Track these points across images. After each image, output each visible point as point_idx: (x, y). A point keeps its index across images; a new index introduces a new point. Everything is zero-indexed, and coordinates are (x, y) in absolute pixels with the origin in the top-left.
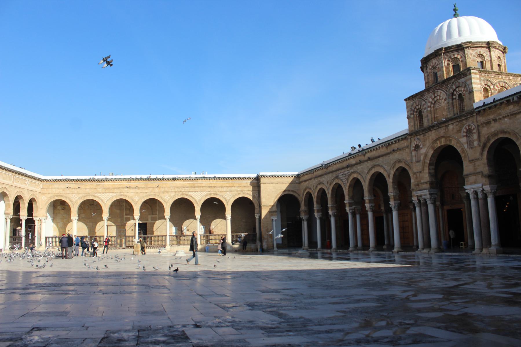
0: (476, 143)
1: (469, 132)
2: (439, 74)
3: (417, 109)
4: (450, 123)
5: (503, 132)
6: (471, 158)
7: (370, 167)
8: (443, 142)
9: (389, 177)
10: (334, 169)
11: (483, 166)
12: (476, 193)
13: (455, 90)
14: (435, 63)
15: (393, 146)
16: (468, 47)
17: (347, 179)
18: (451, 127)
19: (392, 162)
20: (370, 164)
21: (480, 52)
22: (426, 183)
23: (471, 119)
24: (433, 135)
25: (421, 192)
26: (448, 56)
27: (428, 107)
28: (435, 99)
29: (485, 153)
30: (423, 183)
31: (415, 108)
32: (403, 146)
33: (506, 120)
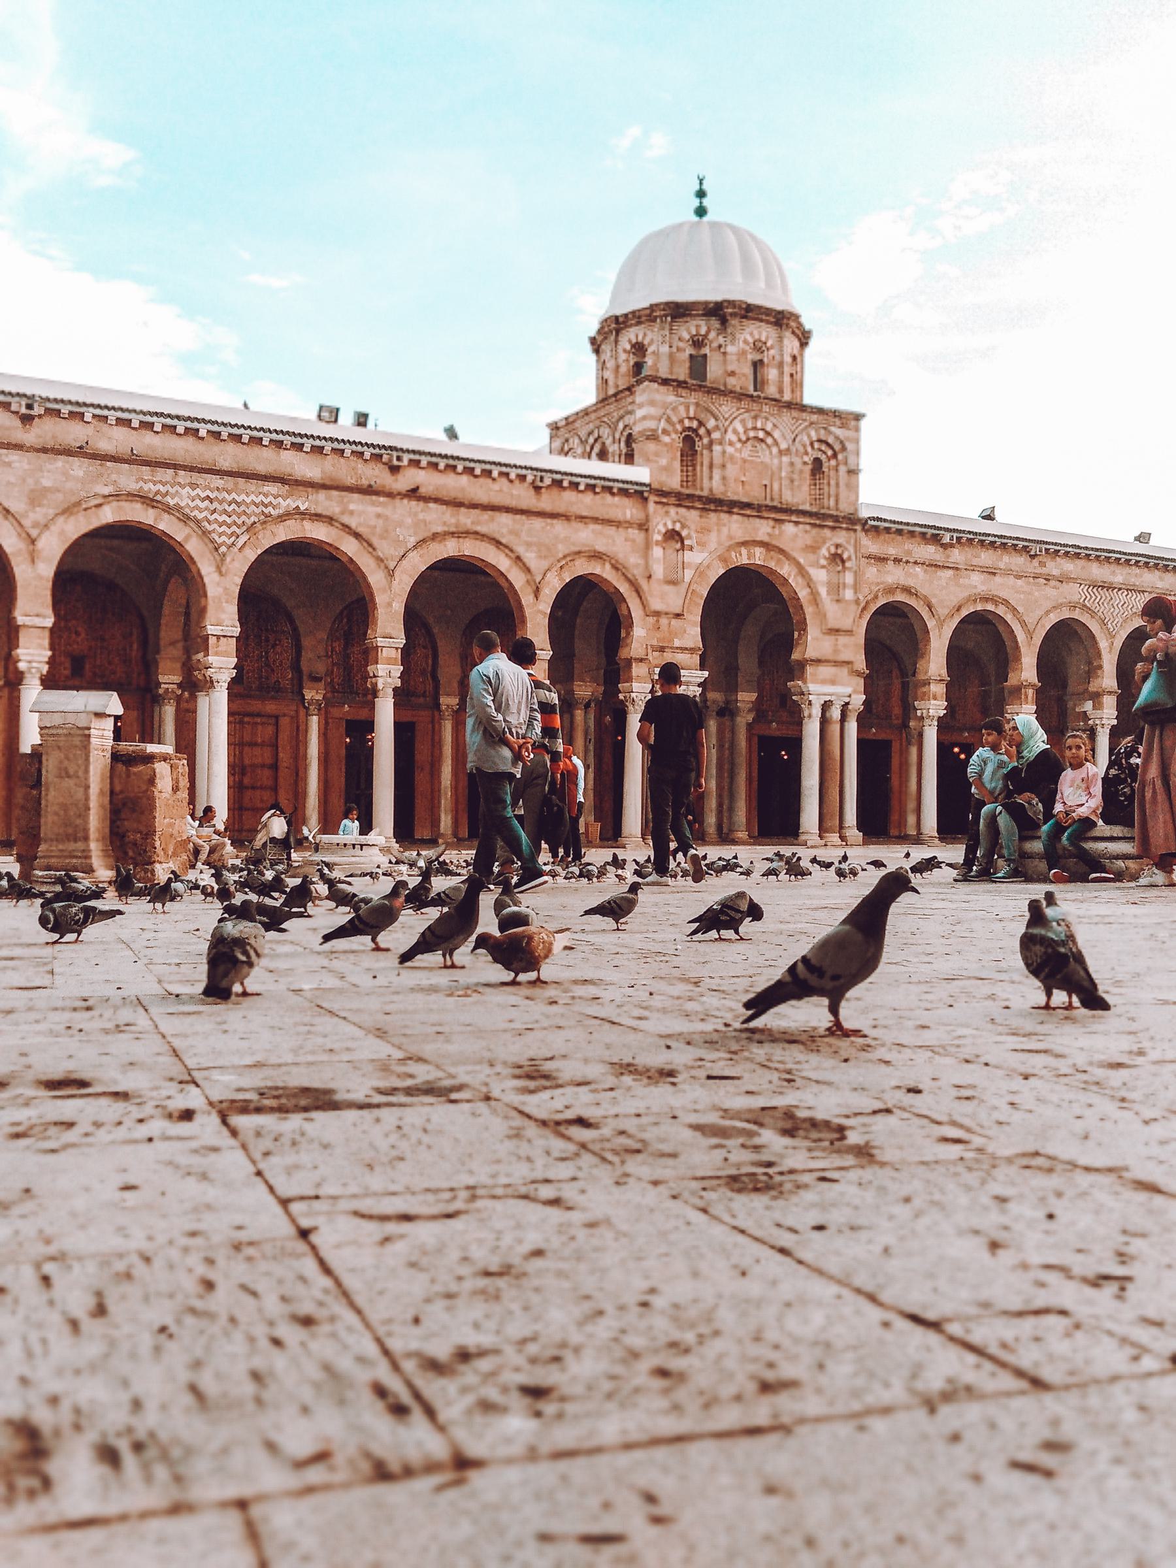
0: (849, 594)
1: (837, 558)
2: (772, 374)
4: (794, 518)
5: (907, 590)
6: (832, 623)
7: (439, 529)
8: (758, 557)
9: (537, 592)
10: (103, 446)
11: (854, 651)
12: (826, 706)
15: (570, 496)
18: (789, 529)
19: (562, 549)
20: (437, 517)
22: (692, 650)
23: (844, 533)
24: (734, 526)
27: (731, 444)
28: (752, 434)
30: (683, 649)
32: (617, 514)
33: (918, 569)
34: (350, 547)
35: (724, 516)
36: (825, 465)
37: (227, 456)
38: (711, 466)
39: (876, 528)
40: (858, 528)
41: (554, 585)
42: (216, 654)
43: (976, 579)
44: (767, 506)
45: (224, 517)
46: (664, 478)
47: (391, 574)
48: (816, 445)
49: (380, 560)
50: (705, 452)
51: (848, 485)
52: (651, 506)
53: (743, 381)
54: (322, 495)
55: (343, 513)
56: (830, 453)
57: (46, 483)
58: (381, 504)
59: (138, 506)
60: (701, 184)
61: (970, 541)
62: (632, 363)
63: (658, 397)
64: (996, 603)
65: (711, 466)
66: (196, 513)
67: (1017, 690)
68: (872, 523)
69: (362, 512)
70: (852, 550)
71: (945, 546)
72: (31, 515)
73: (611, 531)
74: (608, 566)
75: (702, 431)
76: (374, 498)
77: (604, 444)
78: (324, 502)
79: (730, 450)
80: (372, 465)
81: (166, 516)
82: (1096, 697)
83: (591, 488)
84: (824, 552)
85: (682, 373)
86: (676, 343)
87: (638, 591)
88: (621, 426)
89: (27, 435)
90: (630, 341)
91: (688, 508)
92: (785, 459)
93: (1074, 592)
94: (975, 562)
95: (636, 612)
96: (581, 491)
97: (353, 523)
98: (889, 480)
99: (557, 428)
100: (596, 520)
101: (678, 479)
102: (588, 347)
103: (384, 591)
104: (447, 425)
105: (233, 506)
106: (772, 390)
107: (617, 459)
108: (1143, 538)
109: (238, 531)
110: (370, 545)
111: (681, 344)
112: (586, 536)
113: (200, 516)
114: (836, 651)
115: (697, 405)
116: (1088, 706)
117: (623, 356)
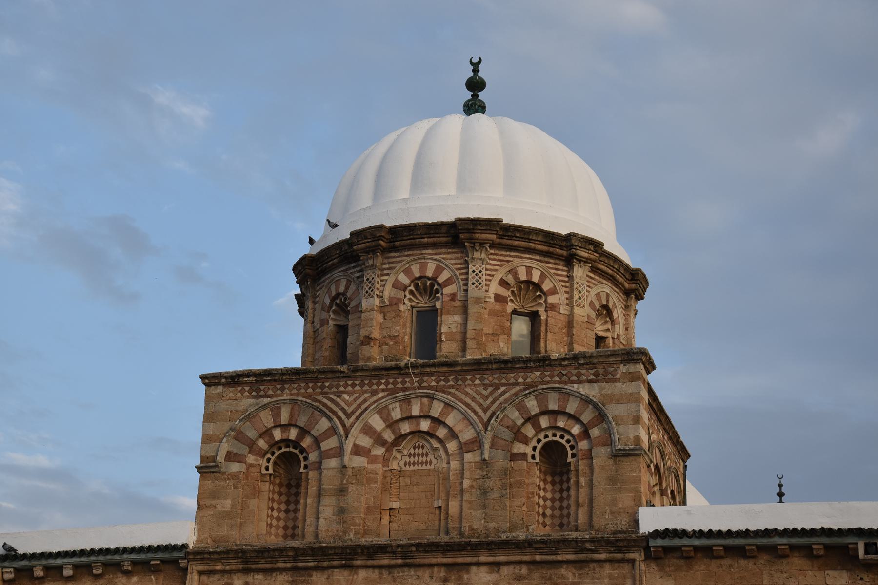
2: (449, 324)
3: (277, 444)
13: (532, 420)
14: (439, 270)
16: (587, 261)
21: (608, 296)
23: (607, 569)
26: (507, 267)
27: (358, 451)
28: (405, 428)
31: (267, 433)
38: (319, 495)
40: (637, 556)
44: (418, 545)
46: (224, 531)
48: (544, 422)
50: (312, 474)
51: (613, 480)
56: (576, 430)
60: (476, 71)
63: (223, 406)
65: (319, 495)
68: (659, 542)
75: (306, 442)
79: (359, 461)
91: (264, 571)
92: (468, 457)
96: (69, 579)
106: (447, 349)
111: (324, 315)
115: (293, 402)
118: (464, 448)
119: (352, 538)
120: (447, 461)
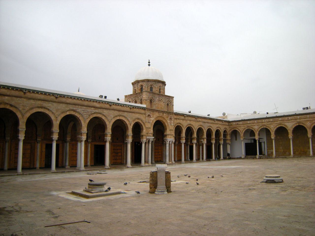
5: (180, 123)
7: (116, 115)
9: (130, 125)
11: (173, 133)
12: (170, 142)
15: (135, 109)
17: (89, 116)
18: (165, 114)
19: (134, 118)
20: (117, 113)
22: (152, 133)
25: (151, 137)
28: (159, 100)
29: (174, 129)
30: (150, 133)
32: (141, 112)
33: (181, 120)
34: (104, 118)
35: (156, 112)
36: (169, 104)
37: (86, 103)
38: (154, 105)
39: (177, 114)
40: (174, 114)
41: (133, 124)
42: (83, 136)
43: (189, 121)
45: (85, 113)
47: (110, 122)
49: (108, 120)
52: (146, 111)
53: (157, 92)
54: (100, 110)
55: (103, 112)
57: (59, 108)
58: (108, 111)
59: (72, 112)
61: (188, 116)
62: (140, 88)
64: (191, 125)
65: (154, 105)
66: (81, 113)
67: (194, 138)
69: (106, 112)
70: (173, 117)
71: (185, 117)
72: (56, 113)
73: (140, 115)
74: (140, 120)
76: (107, 110)
77: (136, 100)
78: (100, 111)
79: (157, 102)
80: (107, 105)
81: (77, 113)
82: (203, 139)
83: (138, 108)
84: (169, 118)
85: (149, 90)
86: (148, 85)
87: (144, 124)
88: (140, 97)
89: (56, 100)
90: (140, 84)
93: (201, 123)
94: (188, 119)
95: (144, 128)
97: (104, 114)
98: (178, 108)
99: (127, 96)
100: (139, 113)
101: (150, 106)
102: (131, 84)
103: (108, 125)
104: (118, 98)
105: (87, 112)
107: (139, 103)
108: (209, 115)
109: (88, 116)
110: (106, 117)
112: (137, 116)
113: (82, 113)
114: (171, 133)
116: (202, 140)
117: (139, 87)
118: (164, 103)
119: (157, 109)
120: (162, 103)
